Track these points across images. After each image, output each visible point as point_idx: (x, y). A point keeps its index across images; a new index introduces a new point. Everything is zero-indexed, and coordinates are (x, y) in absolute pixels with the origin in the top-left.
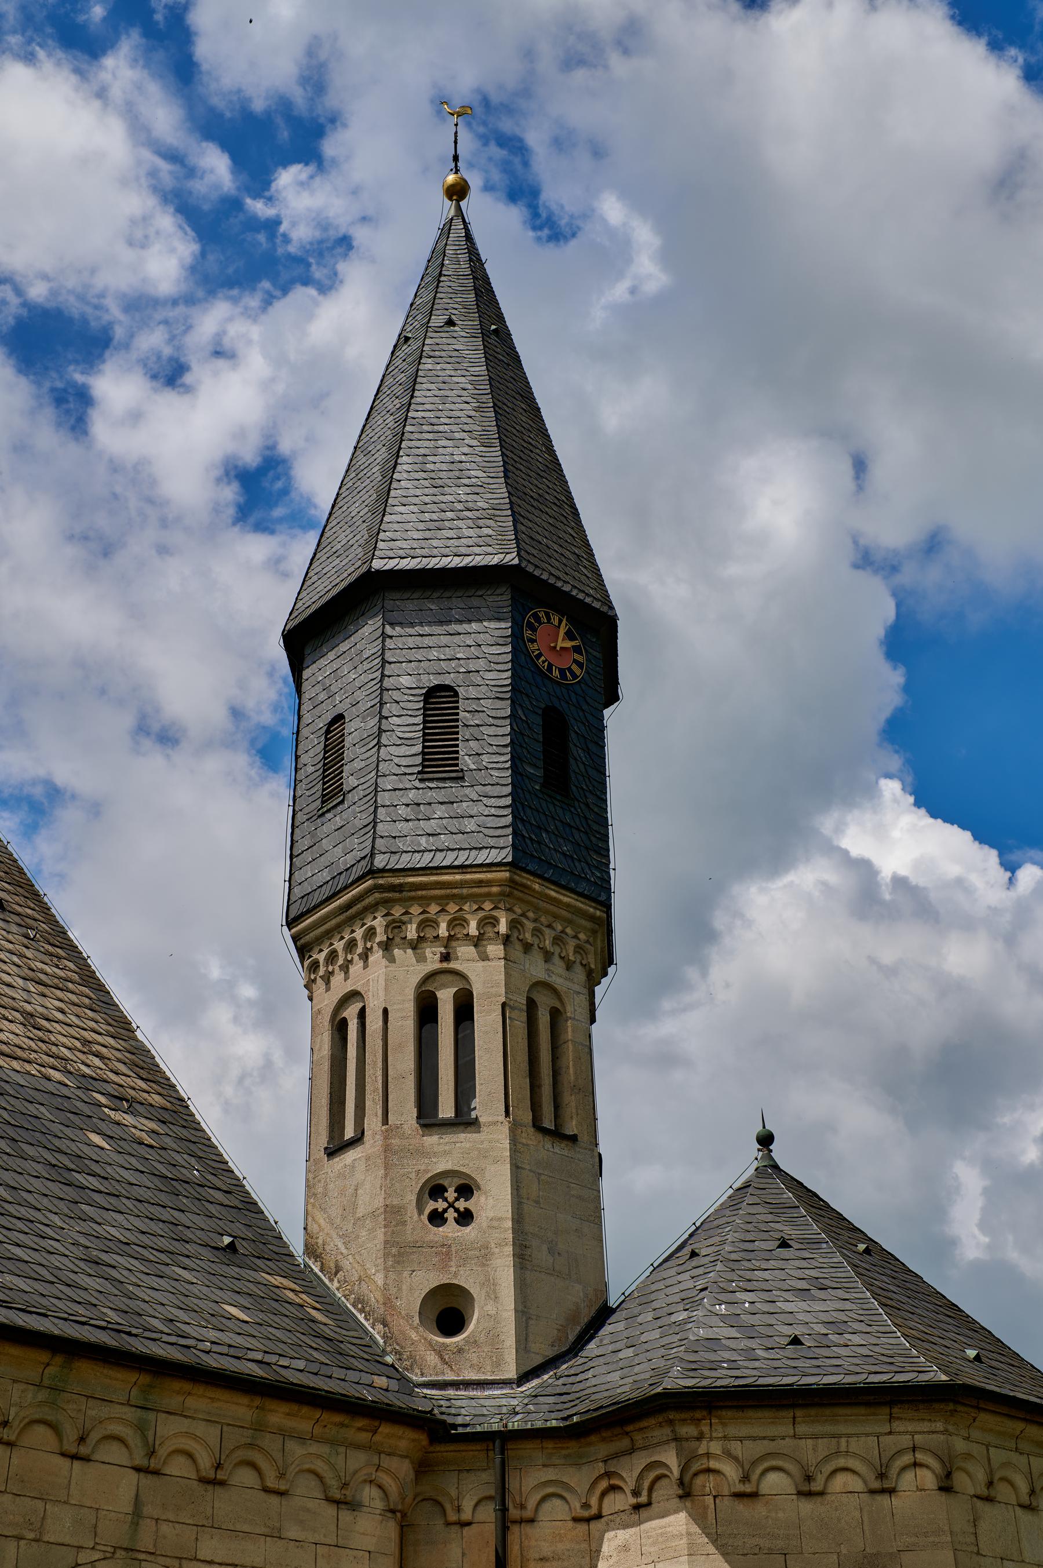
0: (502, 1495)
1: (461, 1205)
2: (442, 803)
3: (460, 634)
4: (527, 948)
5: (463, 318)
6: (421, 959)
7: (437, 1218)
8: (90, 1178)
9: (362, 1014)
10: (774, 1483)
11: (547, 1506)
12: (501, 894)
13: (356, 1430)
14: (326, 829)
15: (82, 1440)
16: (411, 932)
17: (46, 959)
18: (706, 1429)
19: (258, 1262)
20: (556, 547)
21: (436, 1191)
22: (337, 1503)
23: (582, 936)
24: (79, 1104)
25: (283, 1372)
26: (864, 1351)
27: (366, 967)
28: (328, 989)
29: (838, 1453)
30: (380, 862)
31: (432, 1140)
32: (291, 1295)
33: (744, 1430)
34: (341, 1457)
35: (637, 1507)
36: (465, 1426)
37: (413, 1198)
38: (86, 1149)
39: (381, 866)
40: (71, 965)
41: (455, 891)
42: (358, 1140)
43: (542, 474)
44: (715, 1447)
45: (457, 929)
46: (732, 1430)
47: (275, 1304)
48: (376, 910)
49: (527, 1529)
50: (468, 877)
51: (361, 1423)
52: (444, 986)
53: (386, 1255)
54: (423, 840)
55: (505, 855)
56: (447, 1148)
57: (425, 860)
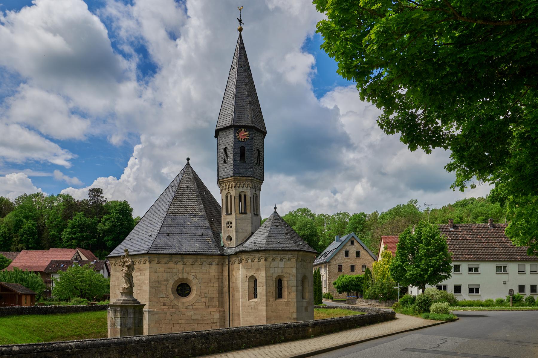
1: (231, 225)
7: (228, 227)
22: (209, 264)
31: (227, 217)
37: (225, 225)
49: (234, 265)
55: (232, 175)
57: (224, 177)
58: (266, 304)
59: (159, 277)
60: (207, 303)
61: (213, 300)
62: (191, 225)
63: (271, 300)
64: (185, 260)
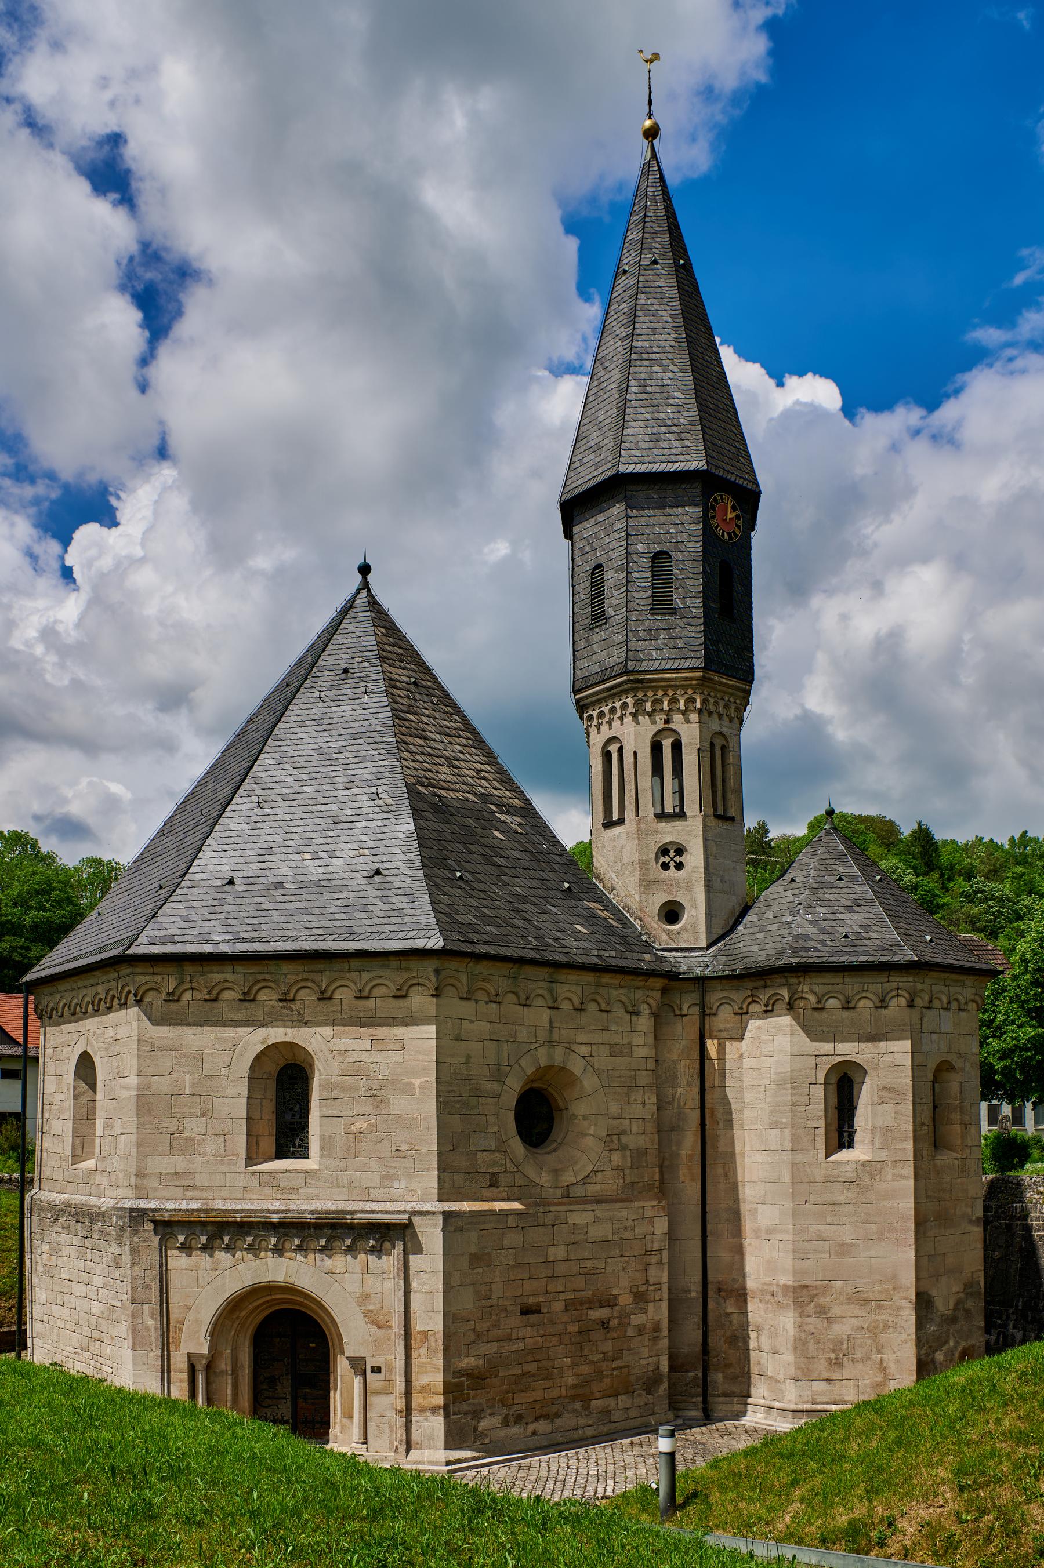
0: (703, 1004)
1: (677, 859)
2: (664, 629)
3: (671, 515)
4: (710, 713)
5: (662, 257)
6: (654, 722)
7: (665, 866)
8: (501, 859)
9: (620, 750)
10: (832, 1003)
11: (722, 1007)
12: (697, 685)
13: (639, 982)
14: (596, 638)
15: (528, 998)
16: (648, 707)
17: (445, 716)
18: (802, 980)
19: (581, 895)
20: (726, 446)
21: (664, 851)
22: (631, 1013)
23: (738, 701)
24: (485, 814)
25: (608, 959)
26: (878, 942)
27: (622, 724)
28: (599, 732)
29: (863, 991)
30: (631, 665)
31: (662, 825)
32: (599, 912)
33: (820, 981)
34: (632, 994)
35: (766, 1011)
36: (684, 973)
37: (653, 856)
38: (495, 842)
39: (631, 669)
40: (456, 717)
41: (672, 683)
42: (621, 822)
43: (716, 385)
44: (806, 988)
45: (673, 705)
46: (814, 981)
47: (594, 919)
48: (629, 693)
50: (680, 675)
51: (641, 978)
52: (667, 738)
53: (640, 885)
54: (654, 653)
55: (700, 663)
56: (670, 829)
58: (915, 1167)
59: (472, 1060)
60: (627, 1172)
61: (644, 1158)
62: (509, 844)
63: (925, 1153)
64: (562, 990)
